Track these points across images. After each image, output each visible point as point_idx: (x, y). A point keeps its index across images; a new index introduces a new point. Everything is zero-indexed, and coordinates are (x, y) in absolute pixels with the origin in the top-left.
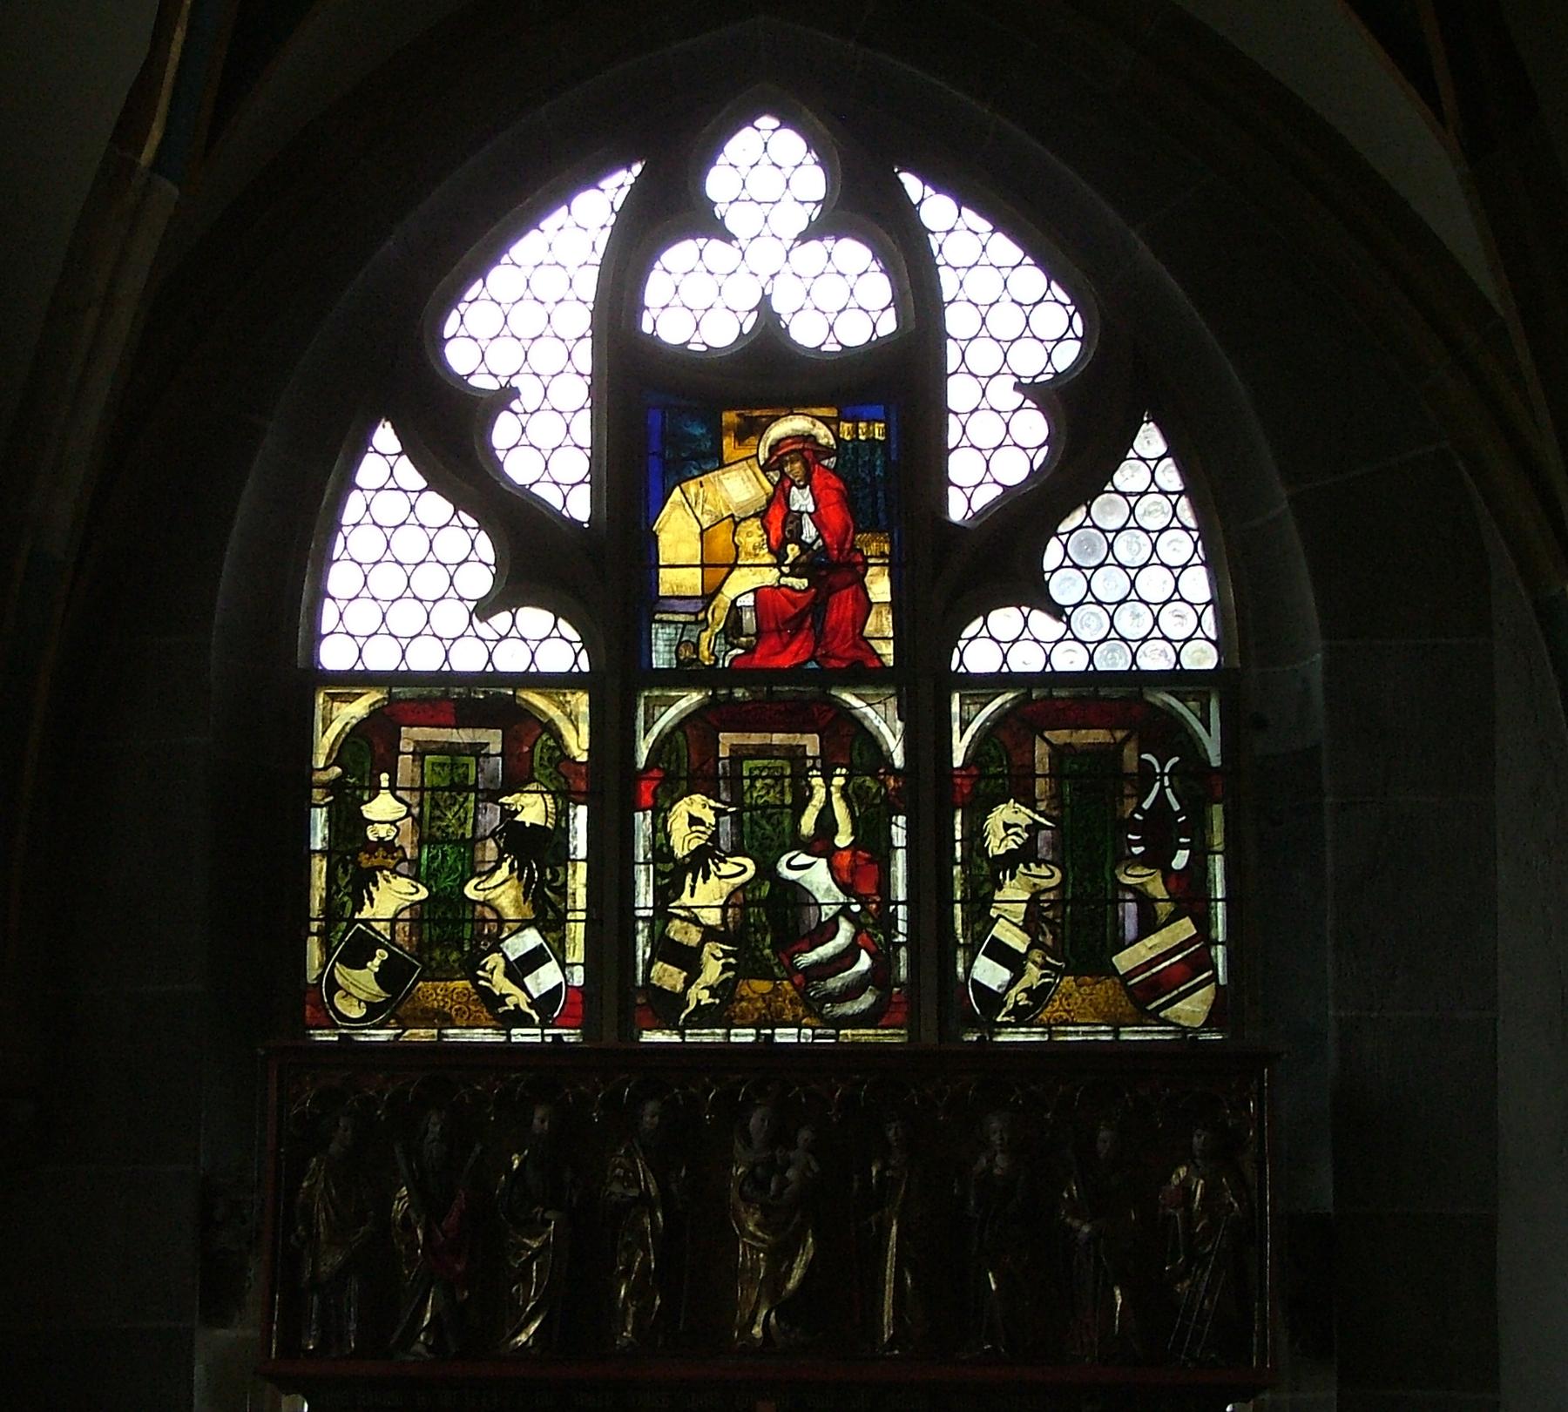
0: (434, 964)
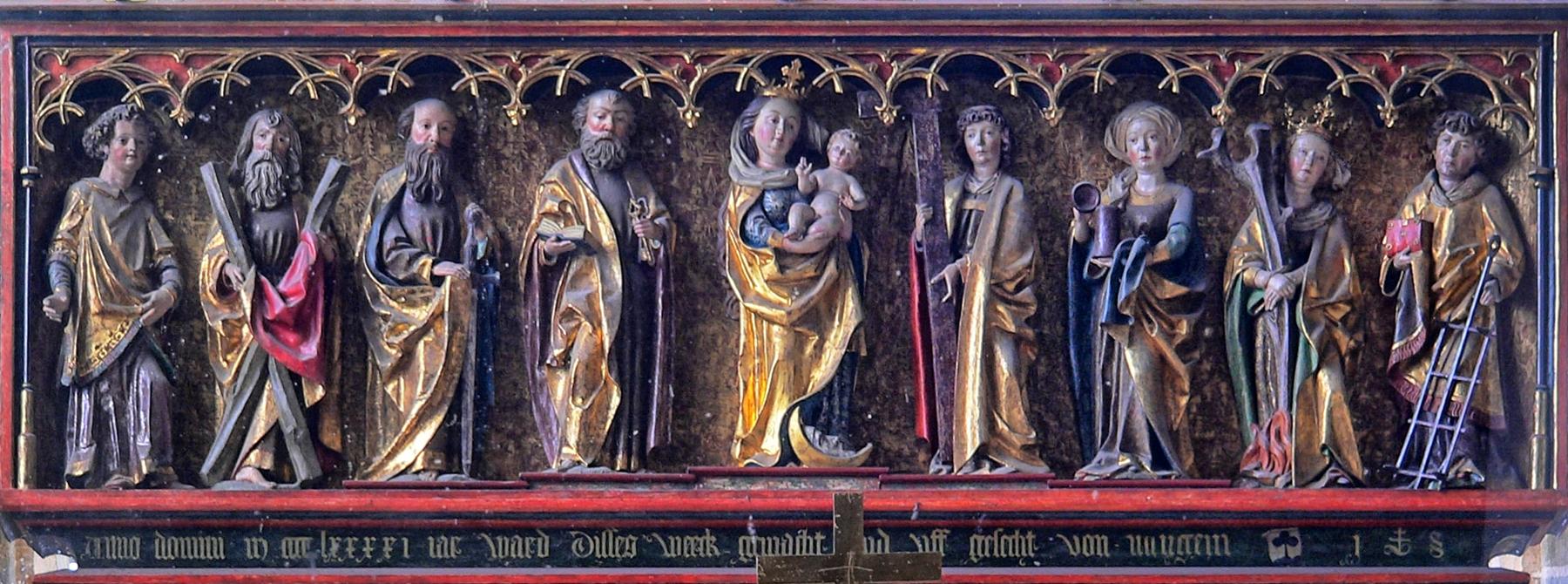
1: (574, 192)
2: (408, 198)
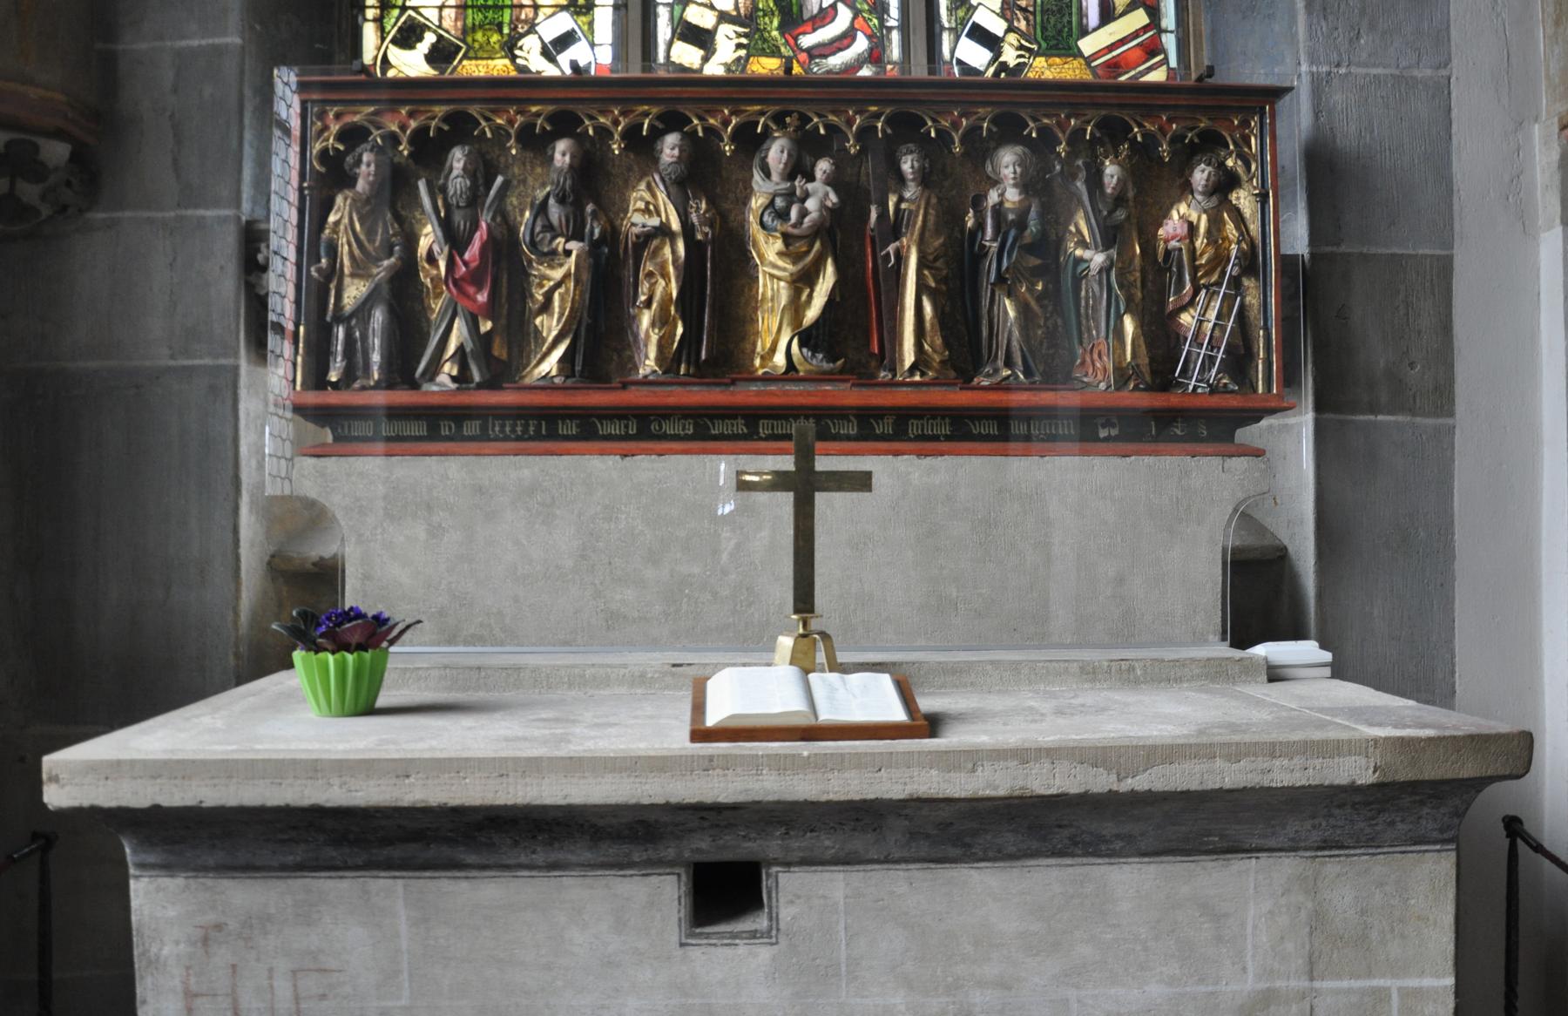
0: (476, 45)
1: (654, 195)
2: (552, 201)
